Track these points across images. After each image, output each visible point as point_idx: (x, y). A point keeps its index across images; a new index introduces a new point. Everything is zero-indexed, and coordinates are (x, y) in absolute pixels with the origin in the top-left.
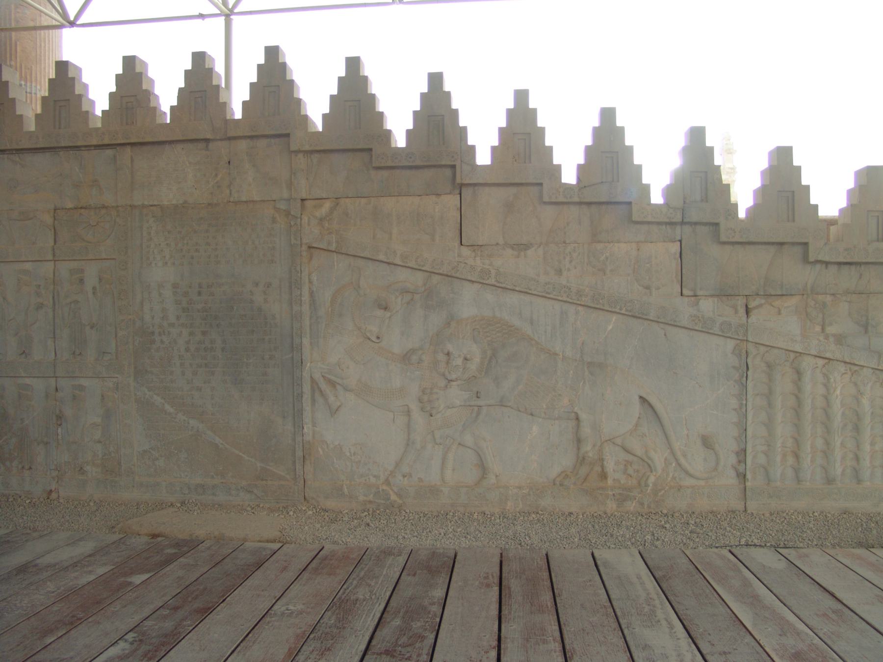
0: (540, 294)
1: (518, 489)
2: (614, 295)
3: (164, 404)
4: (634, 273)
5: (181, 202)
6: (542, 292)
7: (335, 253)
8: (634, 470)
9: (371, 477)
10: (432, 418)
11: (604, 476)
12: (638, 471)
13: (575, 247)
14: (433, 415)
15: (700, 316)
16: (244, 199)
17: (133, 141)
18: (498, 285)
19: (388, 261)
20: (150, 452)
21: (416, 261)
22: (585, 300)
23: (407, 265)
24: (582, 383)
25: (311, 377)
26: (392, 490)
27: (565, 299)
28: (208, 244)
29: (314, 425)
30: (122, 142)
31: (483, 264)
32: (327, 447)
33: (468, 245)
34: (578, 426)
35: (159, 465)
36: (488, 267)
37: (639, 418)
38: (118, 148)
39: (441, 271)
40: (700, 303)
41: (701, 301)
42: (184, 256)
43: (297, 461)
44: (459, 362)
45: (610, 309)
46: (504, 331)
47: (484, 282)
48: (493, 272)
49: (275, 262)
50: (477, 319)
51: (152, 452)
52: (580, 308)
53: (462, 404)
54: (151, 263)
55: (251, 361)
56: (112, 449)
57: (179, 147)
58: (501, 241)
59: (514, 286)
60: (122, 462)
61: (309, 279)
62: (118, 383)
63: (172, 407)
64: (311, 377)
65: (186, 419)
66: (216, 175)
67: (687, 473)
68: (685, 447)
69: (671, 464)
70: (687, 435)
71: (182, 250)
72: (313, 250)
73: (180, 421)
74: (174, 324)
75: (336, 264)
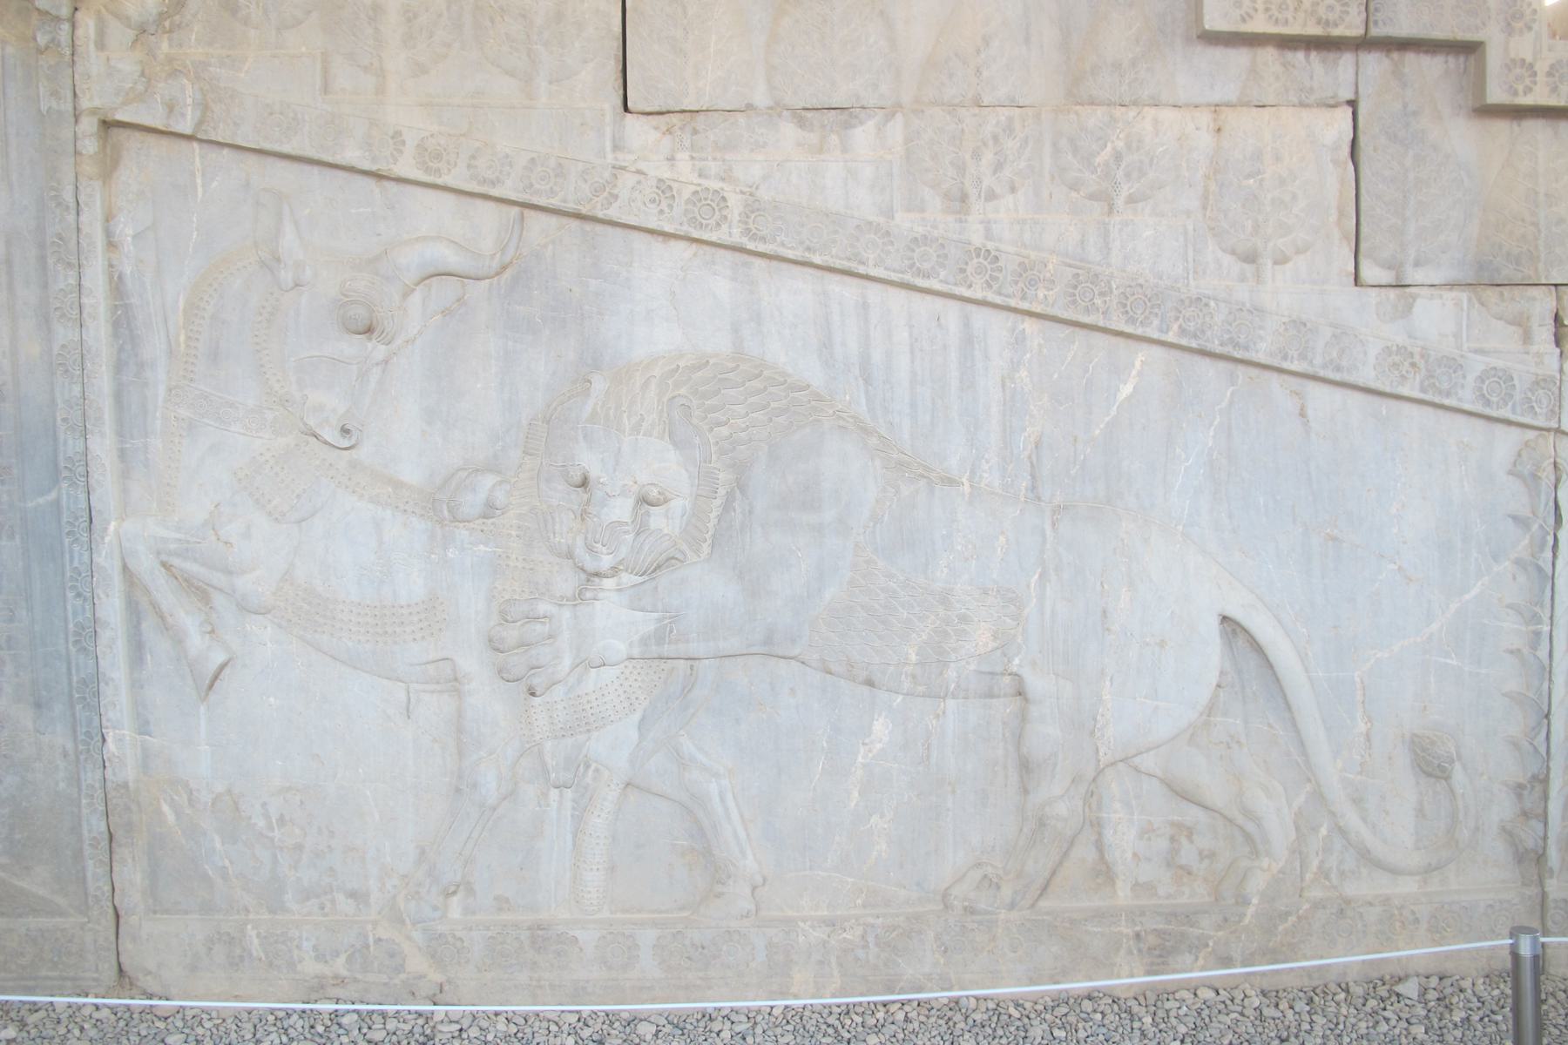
0: (894, 277)
1: (828, 929)
2: (1141, 281)
4: (1204, 208)
6: (902, 272)
7: (195, 145)
8: (1200, 853)
9: (340, 897)
10: (537, 700)
11: (1104, 873)
12: (1212, 855)
13: (1010, 119)
14: (538, 693)
15: (1417, 350)
18: (751, 246)
19: (374, 168)
21: (469, 166)
22: (1045, 296)
23: (439, 181)
24: (1036, 576)
25: (125, 568)
26: (409, 938)
27: (979, 295)
29: (143, 727)
31: (700, 176)
32: (190, 800)
33: (648, 109)
34: (1023, 717)
36: (715, 185)
37: (1219, 686)
39: (554, 202)
40: (1414, 310)
41: (1419, 302)
44: (620, 510)
45: (1129, 329)
46: (773, 405)
47: (705, 237)
48: (735, 202)
50: (682, 364)
52: (1029, 325)
53: (636, 652)
58: (761, 98)
59: (808, 249)
61: (108, 234)
64: (125, 568)
67: (1366, 856)
68: (1361, 773)
69: (1315, 829)
70: (1368, 737)
75: (199, 181)
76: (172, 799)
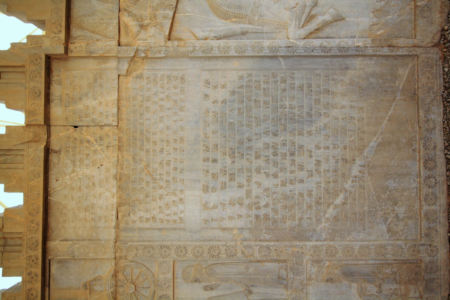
3: (336, 205)
5: (115, 182)
16: (115, 110)
17: (39, 236)
20: (389, 224)
28: (162, 151)
30: (40, 250)
35: (404, 214)
38: (50, 258)
42: (174, 178)
43: (394, 54)
49: (184, 75)
51: (389, 221)
54: (180, 218)
55: (287, 103)
56: (388, 271)
57: (54, 184)
60: (402, 258)
61: (202, 39)
62: (313, 261)
63: (338, 195)
65: (351, 179)
66: (88, 142)
71: (167, 181)
72: (172, 37)
73: (353, 187)
74: (247, 191)
76: (376, 30)
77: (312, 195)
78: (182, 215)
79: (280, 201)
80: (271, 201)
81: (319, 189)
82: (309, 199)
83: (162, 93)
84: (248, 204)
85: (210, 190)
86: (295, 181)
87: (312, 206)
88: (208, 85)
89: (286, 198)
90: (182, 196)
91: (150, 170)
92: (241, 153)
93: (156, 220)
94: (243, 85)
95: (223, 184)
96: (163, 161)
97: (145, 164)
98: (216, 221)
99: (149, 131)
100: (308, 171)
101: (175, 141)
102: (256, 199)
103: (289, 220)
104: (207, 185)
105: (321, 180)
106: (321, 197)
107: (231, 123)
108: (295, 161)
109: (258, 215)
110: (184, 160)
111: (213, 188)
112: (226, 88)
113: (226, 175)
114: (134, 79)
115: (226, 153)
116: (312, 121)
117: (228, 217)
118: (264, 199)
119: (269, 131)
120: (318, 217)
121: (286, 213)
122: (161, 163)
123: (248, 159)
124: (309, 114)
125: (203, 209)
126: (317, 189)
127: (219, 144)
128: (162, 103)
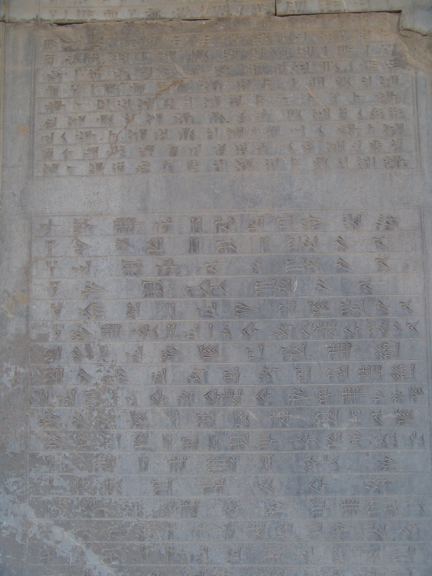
54: (56, 167)
55: (344, 428)
71: (144, 133)
74: (119, 326)
77: (110, 494)
78: (62, 171)
79: (94, 410)
80: (95, 388)
81: (124, 510)
82: (99, 486)
83: (360, 113)
84: (89, 330)
85: (122, 236)
86: (144, 449)
87: (80, 493)
88: (384, 224)
89: (103, 426)
90: (108, 168)
91: (171, 92)
92: (213, 311)
93: (52, 112)
94: (387, 314)
95: (135, 270)
96: (193, 122)
97: (186, 81)
98: (46, 252)
99: (264, 86)
100: (170, 483)
101: (243, 150)
102: (98, 351)
103: (48, 433)
104: (133, 227)
105: (147, 517)
106: (103, 516)
107: (290, 285)
108: (196, 448)
109: (60, 355)
110: (196, 171)
111: (128, 244)
112: (379, 270)
113: (159, 274)
114: (391, 49)
115: (213, 273)
116: (298, 493)
117: (58, 280)
118: (100, 371)
119: (271, 382)
120: (54, 508)
121: (64, 426)
122: (186, 117)
123: (198, 328)
124: (316, 485)
125: (76, 221)
126: (123, 507)
127: (235, 255)
128: (334, 115)
